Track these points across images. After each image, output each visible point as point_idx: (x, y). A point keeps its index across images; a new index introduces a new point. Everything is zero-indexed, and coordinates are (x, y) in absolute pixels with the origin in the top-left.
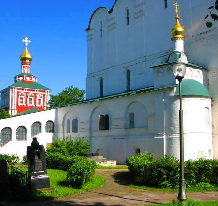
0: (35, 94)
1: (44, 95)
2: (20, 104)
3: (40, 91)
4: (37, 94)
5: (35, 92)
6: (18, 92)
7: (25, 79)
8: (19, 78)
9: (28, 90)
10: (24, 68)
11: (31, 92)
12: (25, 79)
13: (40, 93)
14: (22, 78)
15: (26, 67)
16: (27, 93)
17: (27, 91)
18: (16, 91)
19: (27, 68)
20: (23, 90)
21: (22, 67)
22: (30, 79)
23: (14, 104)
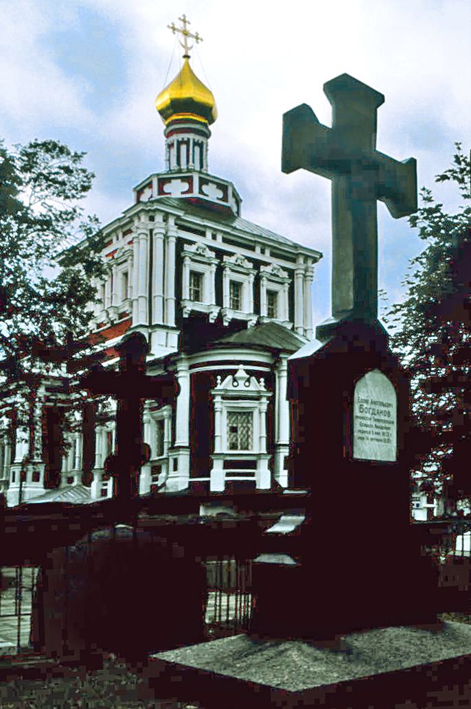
0: (257, 264)
1: (291, 273)
2: (189, 307)
3: (273, 255)
4: (266, 264)
5: (257, 255)
6: (180, 242)
7: (201, 192)
8: (167, 188)
9: (225, 240)
10: (183, 148)
11: (240, 252)
12: (201, 192)
13: (277, 262)
14: (186, 186)
15: (195, 144)
16: (220, 253)
17: (219, 244)
18: (175, 233)
19: (197, 149)
20: (203, 234)
21: (170, 146)
22: (221, 195)
23: (164, 301)
